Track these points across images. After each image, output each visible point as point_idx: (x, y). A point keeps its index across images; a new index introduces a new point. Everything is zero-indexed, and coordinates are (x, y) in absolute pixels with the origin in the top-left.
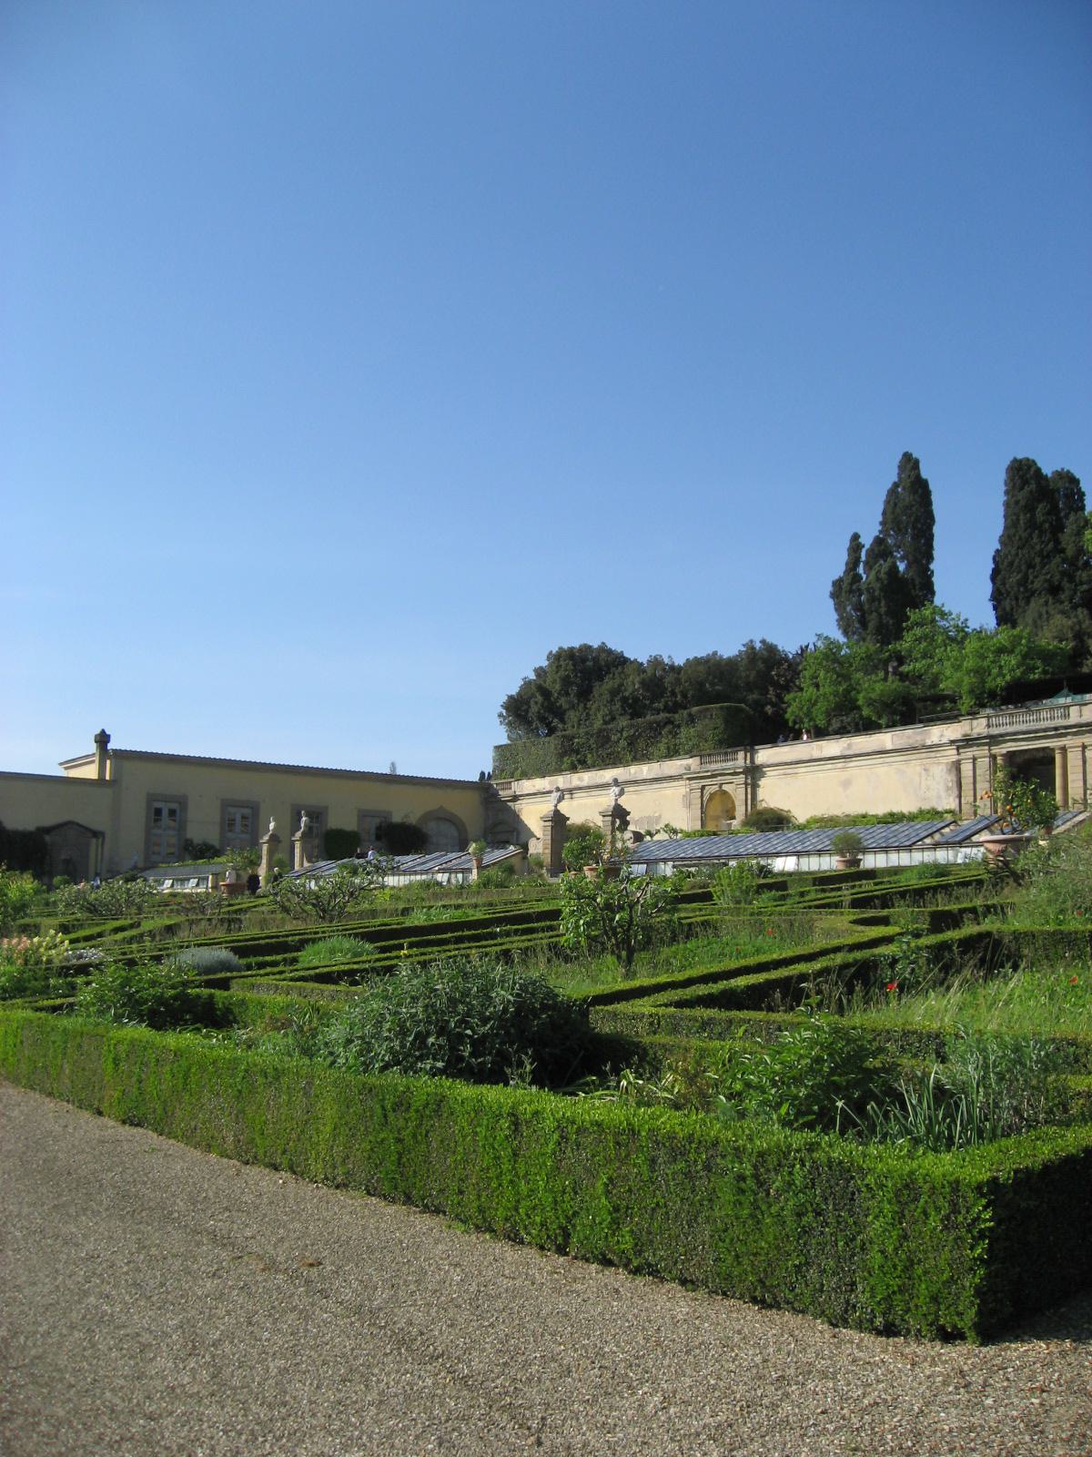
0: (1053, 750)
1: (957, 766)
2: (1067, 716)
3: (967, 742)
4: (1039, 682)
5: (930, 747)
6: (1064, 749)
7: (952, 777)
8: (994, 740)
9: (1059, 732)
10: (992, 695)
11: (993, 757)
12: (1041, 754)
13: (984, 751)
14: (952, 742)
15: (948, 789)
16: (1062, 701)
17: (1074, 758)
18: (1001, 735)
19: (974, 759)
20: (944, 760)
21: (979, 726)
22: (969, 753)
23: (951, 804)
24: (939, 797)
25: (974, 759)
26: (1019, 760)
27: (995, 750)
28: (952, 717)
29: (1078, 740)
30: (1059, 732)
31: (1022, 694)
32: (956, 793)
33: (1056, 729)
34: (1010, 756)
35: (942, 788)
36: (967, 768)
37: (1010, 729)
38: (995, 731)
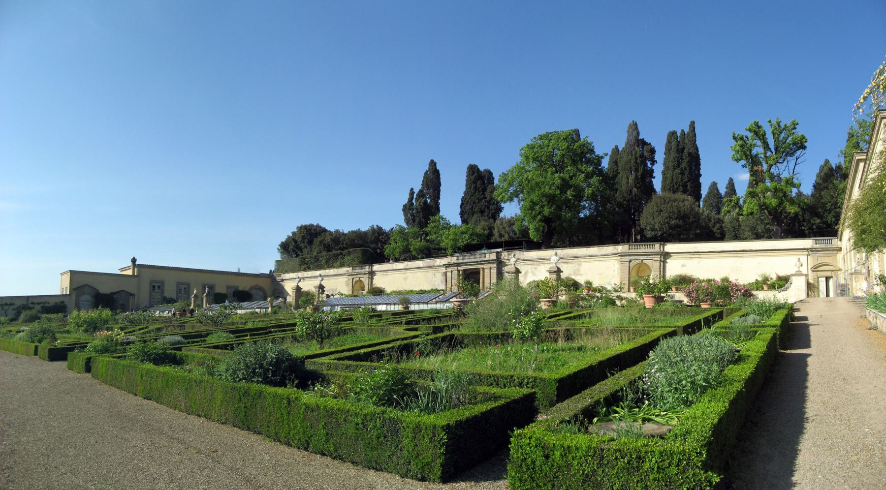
0: (480, 269)
1: (446, 274)
2: (485, 257)
3: (449, 265)
4: (476, 245)
5: (436, 266)
6: (483, 269)
7: (444, 278)
8: (459, 265)
9: (482, 263)
10: (459, 249)
11: (459, 271)
12: (475, 270)
13: (455, 268)
14: (444, 265)
15: (442, 282)
16: (483, 251)
17: (487, 272)
18: (463, 263)
19: (452, 271)
20: (441, 271)
21: (454, 260)
22: (450, 269)
23: (444, 288)
24: (439, 285)
25: (452, 271)
26: (467, 272)
27: (459, 268)
28: (445, 256)
29: (488, 266)
30: (482, 263)
31: (469, 248)
32: (445, 283)
33: (481, 261)
34: (465, 271)
35: (440, 281)
36: (449, 274)
37: (465, 261)
38: (459, 262)
